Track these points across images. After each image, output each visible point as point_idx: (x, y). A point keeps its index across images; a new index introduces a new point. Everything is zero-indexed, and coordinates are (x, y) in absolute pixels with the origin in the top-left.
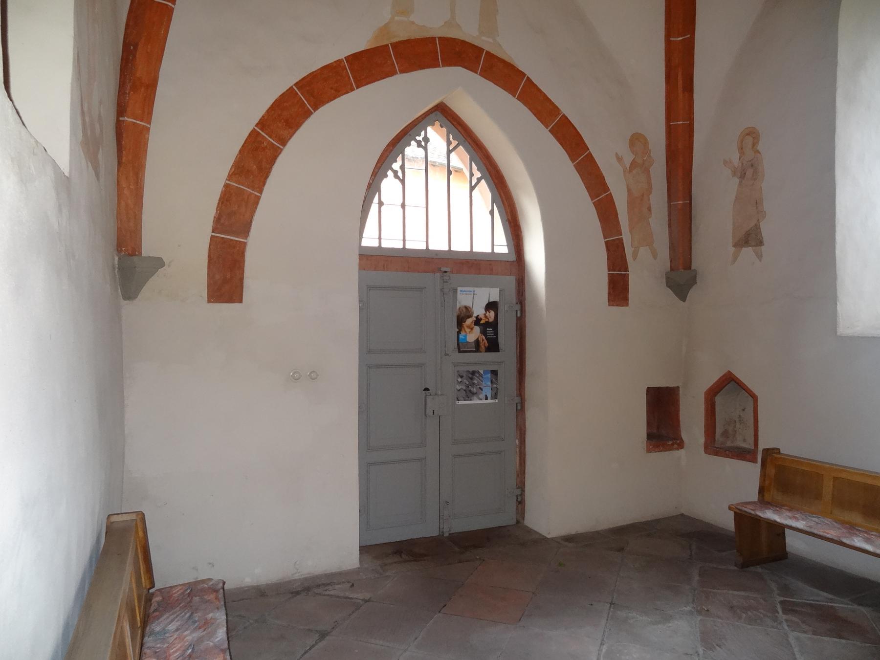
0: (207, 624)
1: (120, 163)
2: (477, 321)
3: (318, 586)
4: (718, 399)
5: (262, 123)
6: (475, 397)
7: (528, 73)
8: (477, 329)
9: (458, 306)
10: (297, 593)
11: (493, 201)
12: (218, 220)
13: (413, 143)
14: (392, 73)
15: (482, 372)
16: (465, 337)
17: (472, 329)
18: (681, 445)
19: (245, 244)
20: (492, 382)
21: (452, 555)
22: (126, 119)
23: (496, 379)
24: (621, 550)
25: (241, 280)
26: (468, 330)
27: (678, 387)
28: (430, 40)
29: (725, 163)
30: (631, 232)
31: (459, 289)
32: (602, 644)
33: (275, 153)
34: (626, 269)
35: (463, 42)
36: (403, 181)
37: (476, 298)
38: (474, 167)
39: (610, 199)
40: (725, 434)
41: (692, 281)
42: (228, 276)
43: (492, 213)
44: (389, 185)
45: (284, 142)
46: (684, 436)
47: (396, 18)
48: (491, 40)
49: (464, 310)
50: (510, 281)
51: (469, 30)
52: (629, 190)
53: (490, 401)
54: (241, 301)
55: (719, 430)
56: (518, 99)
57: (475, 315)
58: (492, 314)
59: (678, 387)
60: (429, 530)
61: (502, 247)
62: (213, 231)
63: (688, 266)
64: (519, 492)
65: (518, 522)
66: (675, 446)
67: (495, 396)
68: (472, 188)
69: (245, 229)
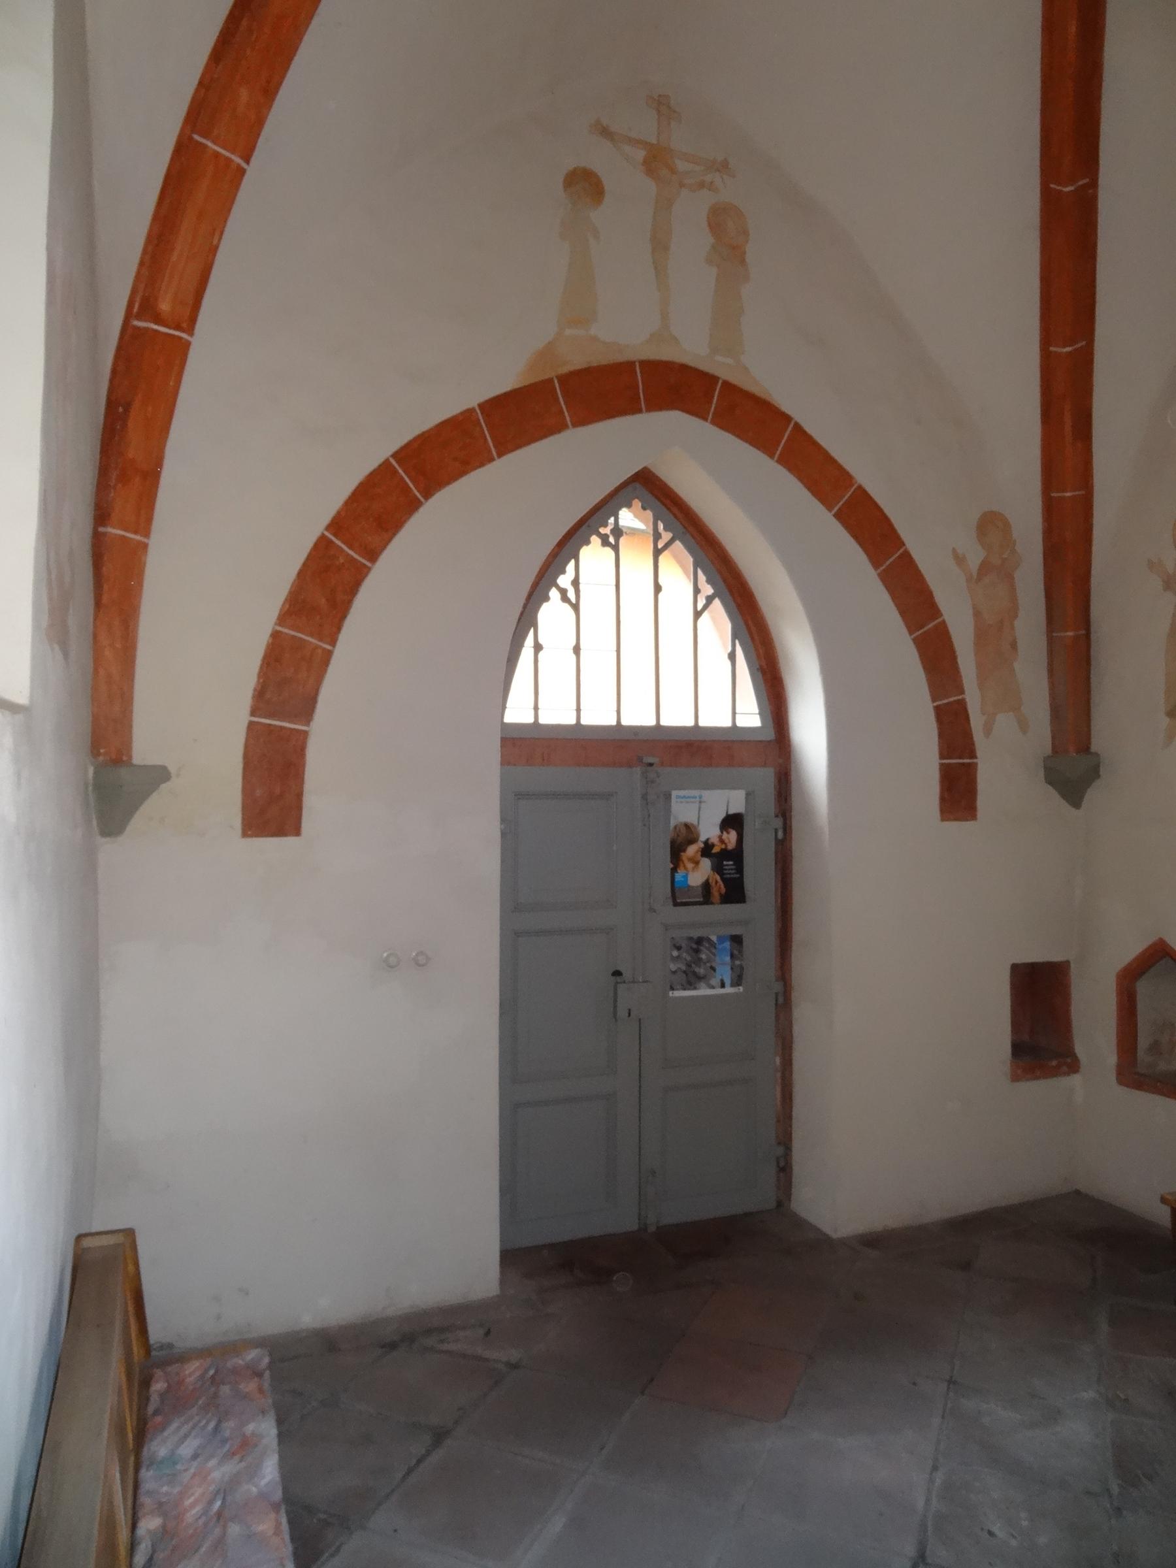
0: (246, 1445)
1: (98, 604)
2: (707, 850)
3: (429, 1332)
4: (1143, 988)
5: (337, 525)
6: (703, 984)
7: (798, 415)
9: (673, 823)
10: (392, 1346)
11: (735, 636)
12: (260, 695)
13: (595, 540)
14: (559, 428)
15: (714, 938)
16: (686, 877)
17: (697, 863)
18: (1073, 1066)
19: (306, 733)
20: (732, 956)
21: (659, 1269)
22: (110, 530)
23: (740, 952)
24: (966, 1266)
25: (299, 796)
26: (690, 866)
27: (1068, 962)
28: (627, 367)
29: (1151, 565)
30: (981, 686)
31: (674, 793)
32: (935, 1468)
33: (358, 575)
34: (973, 755)
35: (684, 368)
36: (576, 607)
37: (705, 809)
38: (702, 577)
39: (943, 633)
40: (1155, 1047)
41: (1093, 773)
42: (278, 791)
43: (732, 657)
44: (552, 614)
45: (373, 555)
46: (1080, 1049)
47: (568, 332)
48: (730, 361)
49: (683, 830)
50: (765, 777)
51: (692, 346)
52: (977, 614)
53: (728, 990)
54: (297, 831)
55: (1143, 1042)
56: (779, 461)
57: (703, 838)
58: (732, 837)
59: (1068, 962)
60: (620, 1218)
61: (750, 716)
62: (253, 713)
63: (1085, 748)
64: (780, 1151)
65: (779, 1204)
66: (1065, 1068)
67: (738, 981)
68: (697, 614)
69: (306, 708)
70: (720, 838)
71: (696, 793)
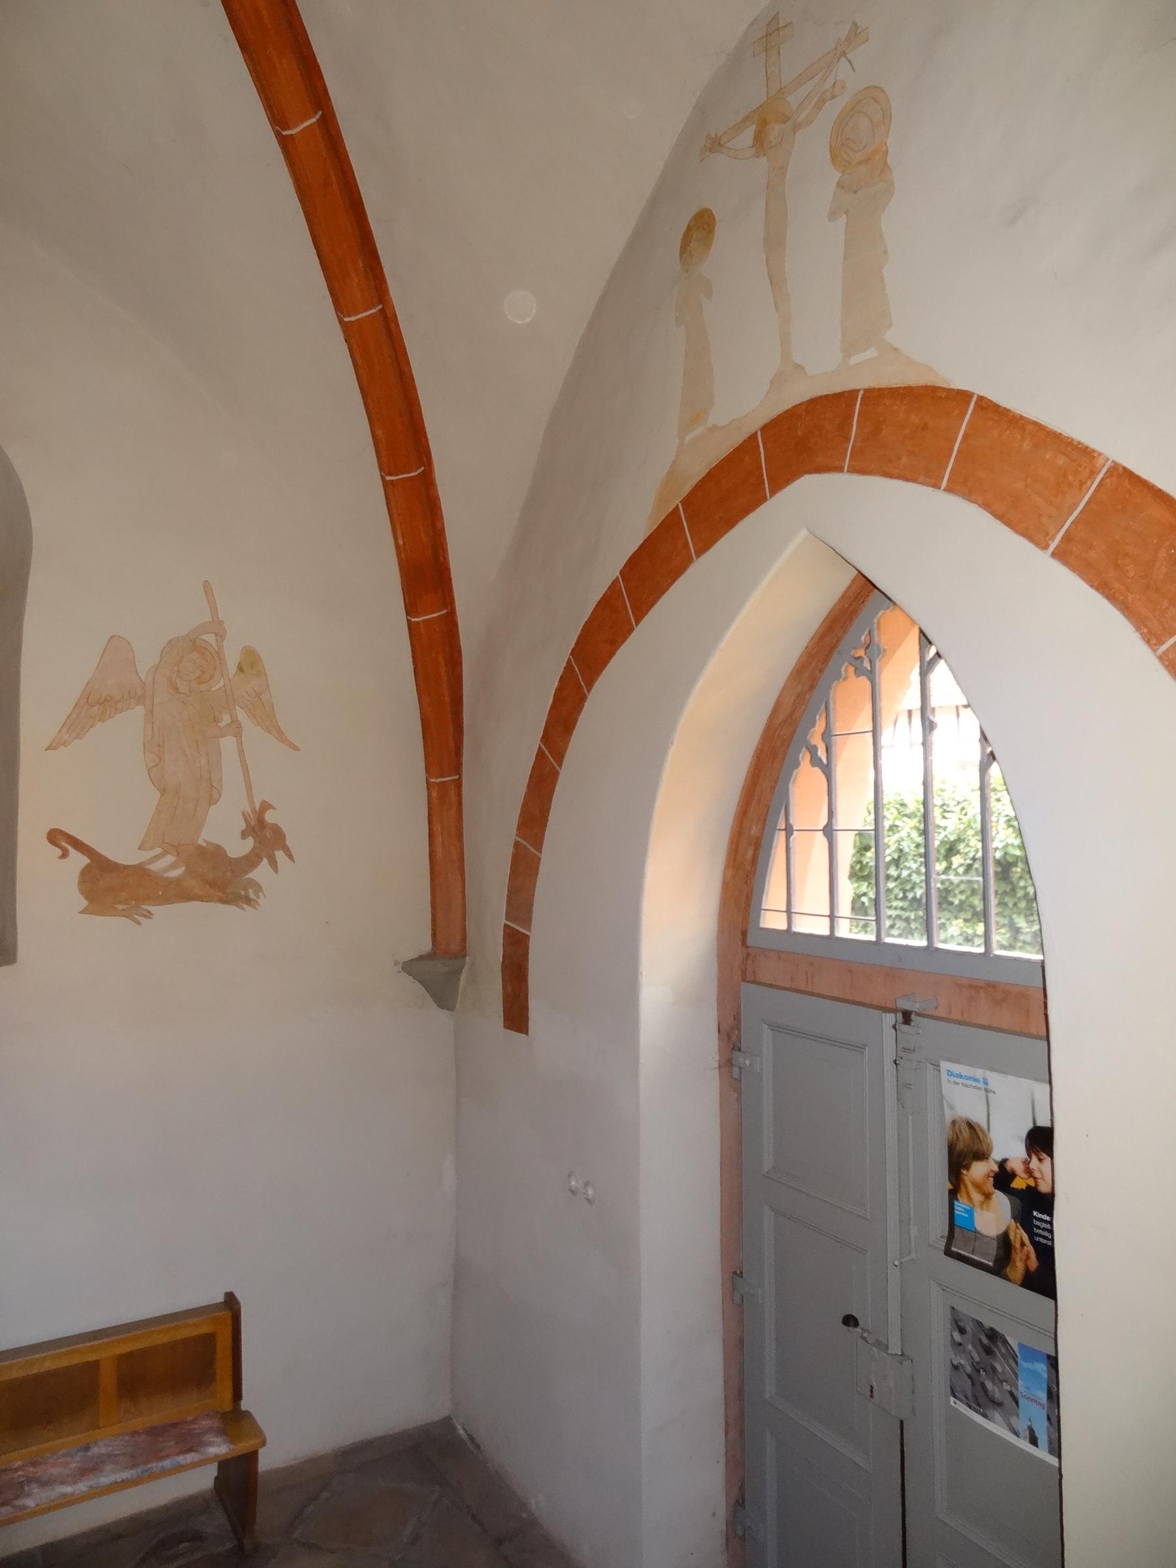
2: (1003, 1178)
8: (1001, 1201)
9: (949, 1116)
13: (848, 670)
16: (971, 1213)
17: (988, 1196)
26: (977, 1197)
31: (945, 1065)
48: (872, 353)
49: (966, 1133)
57: (997, 1155)
70: (1026, 1163)
71: (979, 1073)
